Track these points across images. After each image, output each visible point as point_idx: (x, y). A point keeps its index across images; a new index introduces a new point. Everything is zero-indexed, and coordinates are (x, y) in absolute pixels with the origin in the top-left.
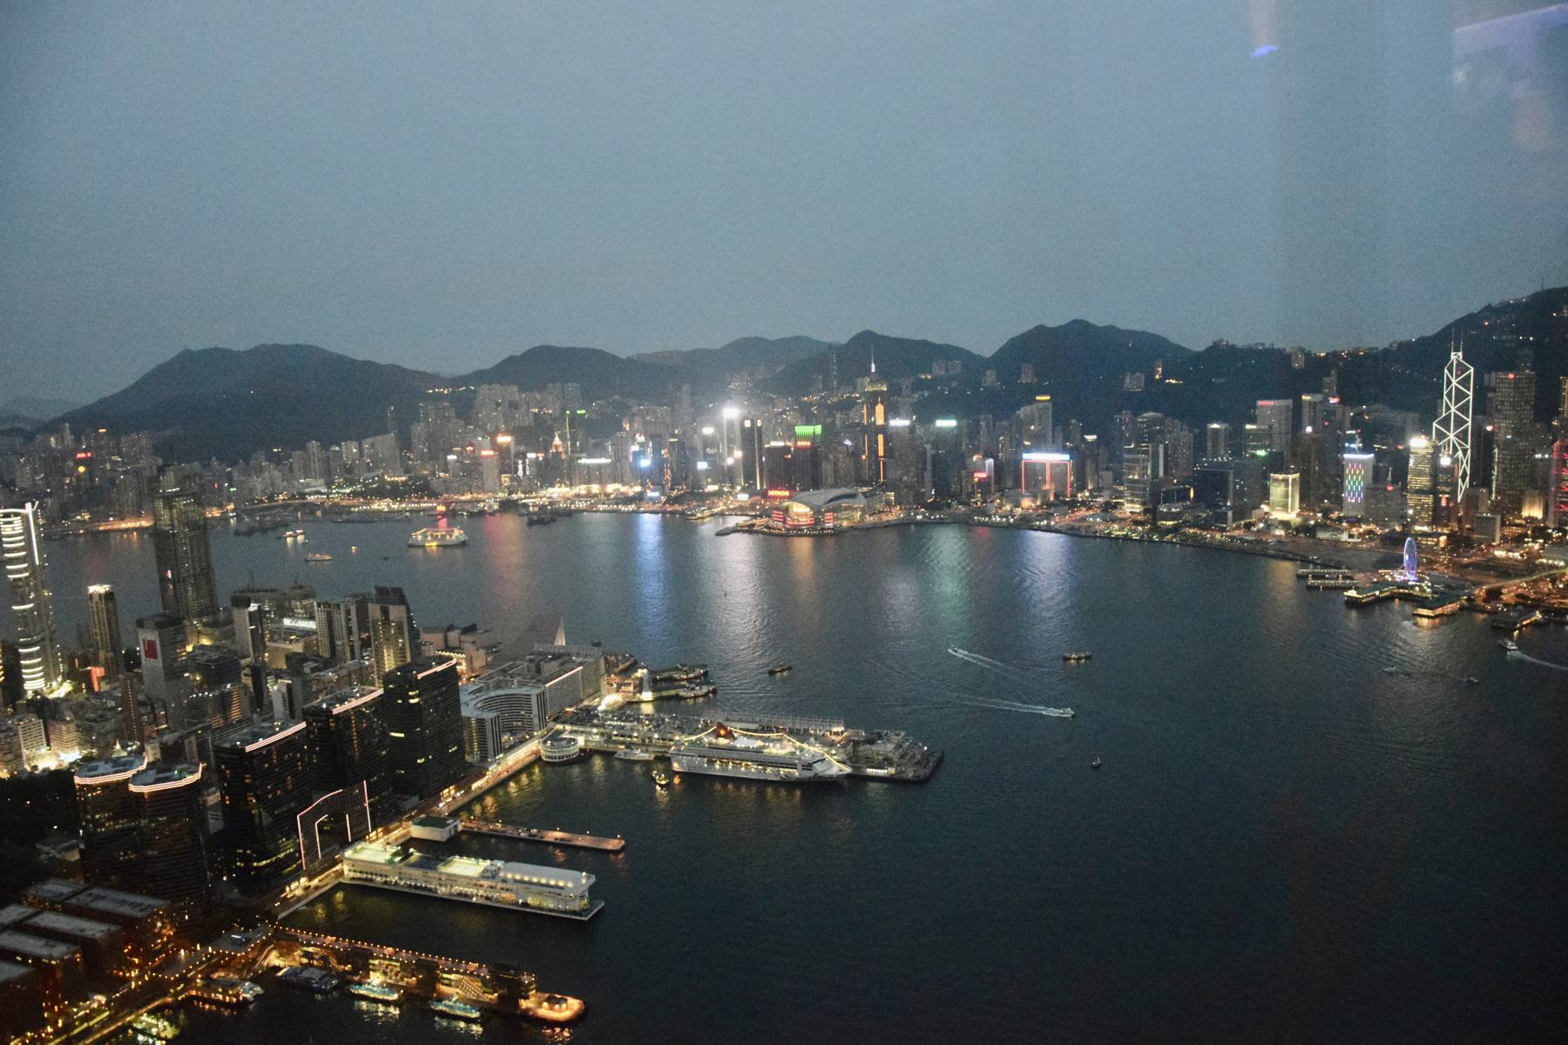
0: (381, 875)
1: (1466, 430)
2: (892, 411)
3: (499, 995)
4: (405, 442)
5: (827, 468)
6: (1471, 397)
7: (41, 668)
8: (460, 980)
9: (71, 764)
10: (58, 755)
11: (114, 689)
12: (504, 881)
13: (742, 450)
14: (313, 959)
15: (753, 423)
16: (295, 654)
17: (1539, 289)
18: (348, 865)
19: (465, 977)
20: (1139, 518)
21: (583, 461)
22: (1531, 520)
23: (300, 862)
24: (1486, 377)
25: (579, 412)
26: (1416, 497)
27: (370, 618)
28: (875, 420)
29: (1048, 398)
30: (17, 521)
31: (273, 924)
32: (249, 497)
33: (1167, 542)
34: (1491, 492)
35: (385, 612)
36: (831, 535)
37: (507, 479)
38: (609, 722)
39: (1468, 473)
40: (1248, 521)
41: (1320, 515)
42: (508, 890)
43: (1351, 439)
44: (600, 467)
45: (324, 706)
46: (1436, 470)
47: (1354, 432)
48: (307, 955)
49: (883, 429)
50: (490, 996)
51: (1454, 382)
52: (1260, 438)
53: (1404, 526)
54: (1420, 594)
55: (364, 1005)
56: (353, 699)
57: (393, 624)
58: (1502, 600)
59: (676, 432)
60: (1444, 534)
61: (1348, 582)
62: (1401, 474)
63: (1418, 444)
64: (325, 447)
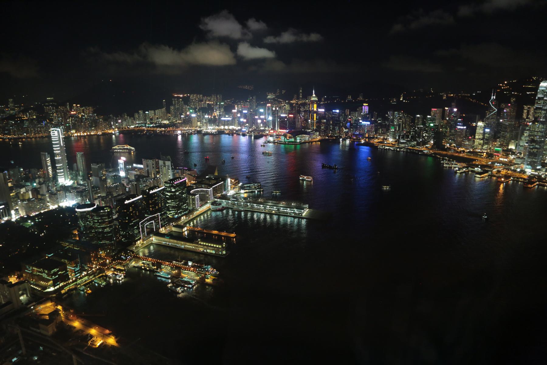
0: (164, 241)
2: (318, 107)
3: (200, 278)
4: (168, 111)
5: (299, 124)
7: (63, 176)
8: (188, 273)
9: (73, 205)
10: (69, 202)
11: (85, 183)
12: (201, 245)
13: (272, 117)
14: (145, 264)
15: (276, 109)
16: (137, 175)
18: (154, 238)
19: (190, 272)
20: (393, 143)
21: (223, 119)
23: (140, 237)
25: (222, 103)
26: (478, 141)
27: (160, 165)
28: (313, 109)
29: (367, 104)
30: (56, 133)
31: (133, 254)
32: (122, 127)
33: (402, 151)
35: (164, 163)
36: (299, 144)
37: (199, 124)
38: (231, 199)
40: (427, 146)
41: (448, 145)
42: (201, 247)
43: (459, 122)
44: (228, 121)
45: (147, 191)
46: (484, 133)
48: (143, 263)
49: (317, 112)
50: (197, 278)
52: (433, 120)
53: (473, 150)
54: (477, 170)
55: (159, 278)
56: (156, 189)
57: (167, 167)
58: (501, 173)
59: (251, 110)
60: (485, 152)
61: (456, 166)
63: (480, 124)
64: (144, 112)
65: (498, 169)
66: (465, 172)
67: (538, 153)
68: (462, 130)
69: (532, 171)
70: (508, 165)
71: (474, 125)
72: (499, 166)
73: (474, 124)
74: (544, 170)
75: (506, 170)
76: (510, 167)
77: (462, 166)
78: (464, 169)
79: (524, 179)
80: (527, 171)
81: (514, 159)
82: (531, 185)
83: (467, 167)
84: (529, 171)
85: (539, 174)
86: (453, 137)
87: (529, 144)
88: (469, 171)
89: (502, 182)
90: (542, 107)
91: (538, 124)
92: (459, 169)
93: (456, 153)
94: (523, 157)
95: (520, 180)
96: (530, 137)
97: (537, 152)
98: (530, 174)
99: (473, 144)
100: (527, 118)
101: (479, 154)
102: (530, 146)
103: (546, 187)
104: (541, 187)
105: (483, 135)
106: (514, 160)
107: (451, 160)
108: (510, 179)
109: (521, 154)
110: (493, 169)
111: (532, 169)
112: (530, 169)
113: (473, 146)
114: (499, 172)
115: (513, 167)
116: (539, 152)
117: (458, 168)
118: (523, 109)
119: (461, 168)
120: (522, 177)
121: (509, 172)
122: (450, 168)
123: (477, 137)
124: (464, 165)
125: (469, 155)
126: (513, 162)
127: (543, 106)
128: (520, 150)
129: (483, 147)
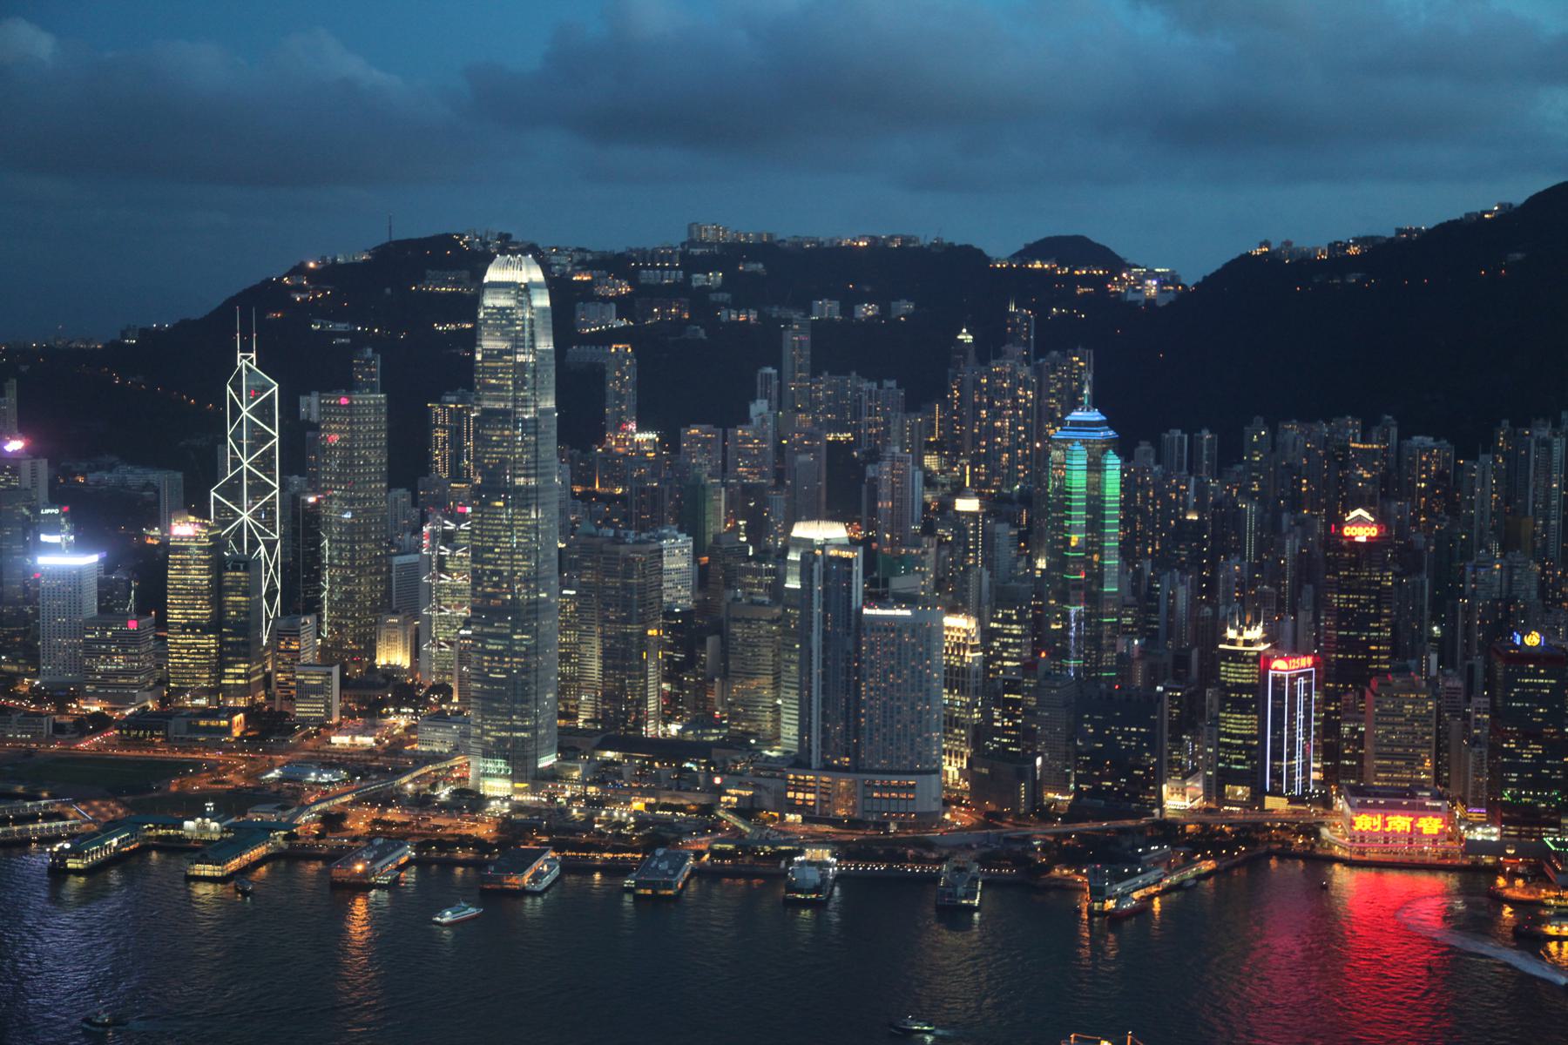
1: (271, 503)
6: (276, 440)
17: (385, 240)
22: (391, 671)
24: (303, 400)
34: (319, 620)
39: (279, 586)
43: (54, 527)
46: (217, 591)
47: (56, 511)
51: (245, 412)
53: (164, 701)
58: (346, 829)
60: (235, 711)
62: (153, 597)
63: (184, 529)
65: (324, 805)
66: (117, 859)
67: (532, 679)
68: (74, 580)
69: (517, 791)
70: (381, 771)
71: (149, 541)
72: (330, 783)
73: (153, 535)
74: (576, 775)
75: (373, 806)
76: (397, 783)
77: (94, 822)
78: (115, 842)
79: (479, 844)
80: (489, 793)
81: (409, 729)
82: (521, 870)
83: (132, 825)
84: (499, 788)
85: (551, 798)
86: (14, 634)
87: (479, 629)
88: (144, 850)
89: (361, 886)
90: (510, 405)
91: (506, 506)
92: (81, 842)
93: (51, 739)
94: (459, 713)
95: (460, 854)
96: (479, 589)
97: (525, 670)
98: (507, 811)
99: (159, 666)
100: (457, 474)
101: (203, 723)
102: (484, 643)
103: (597, 876)
104: (573, 878)
105: (211, 602)
106: (413, 737)
107: (20, 789)
108: (403, 860)
109: (444, 690)
110: (294, 810)
111: (513, 778)
112: (505, 776)
113: (158, 674)
114: (332, 821)
115: (413, 781)
116: (536, 670)
117: (70, 838)
118: (425, 425)
119: (95, 834)
120: (469, 836)
121: (393, 814)
122: (16, 851)
123: (175, 615)
124: (113, 810)
125: (138, 743)
126: (408, 748)
127: (515, 400)
128: (443, 671)
129: (222, 675)
